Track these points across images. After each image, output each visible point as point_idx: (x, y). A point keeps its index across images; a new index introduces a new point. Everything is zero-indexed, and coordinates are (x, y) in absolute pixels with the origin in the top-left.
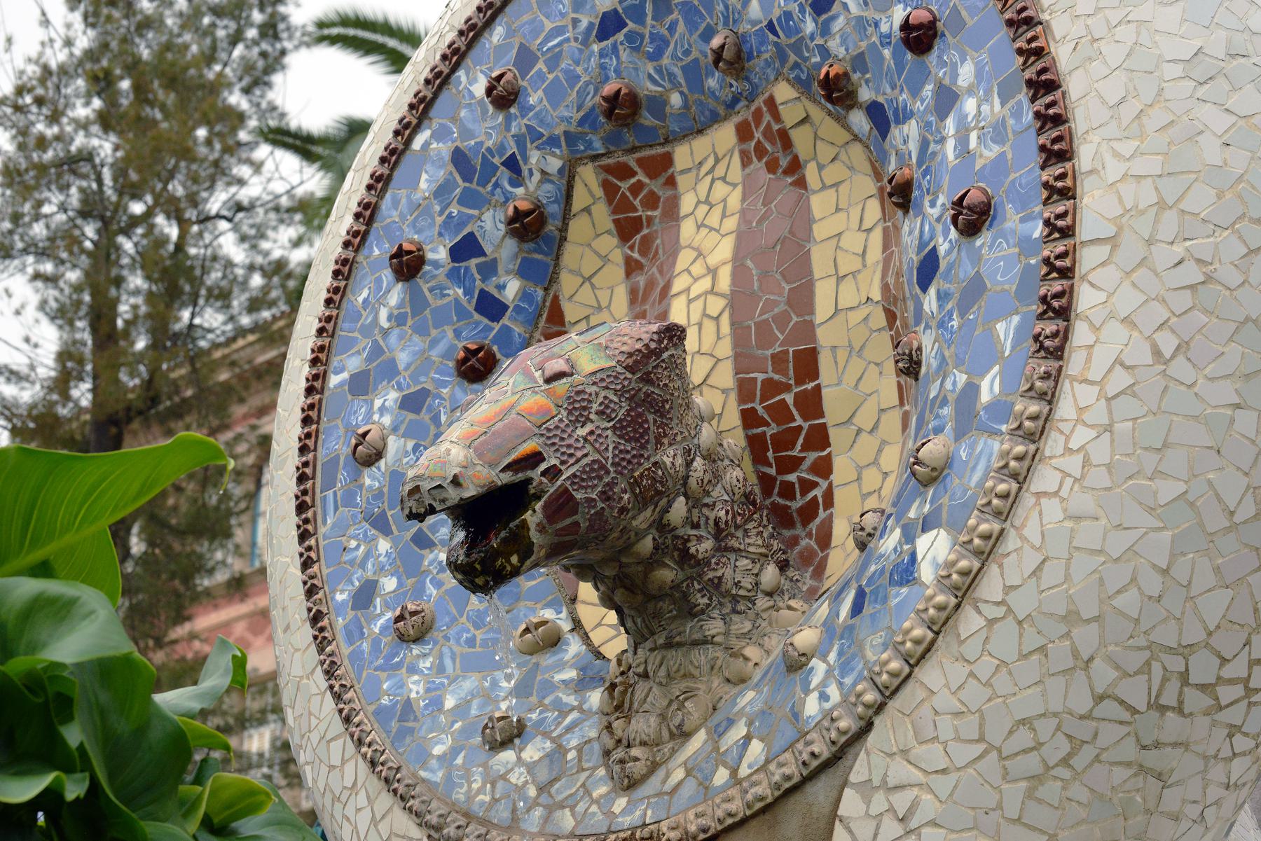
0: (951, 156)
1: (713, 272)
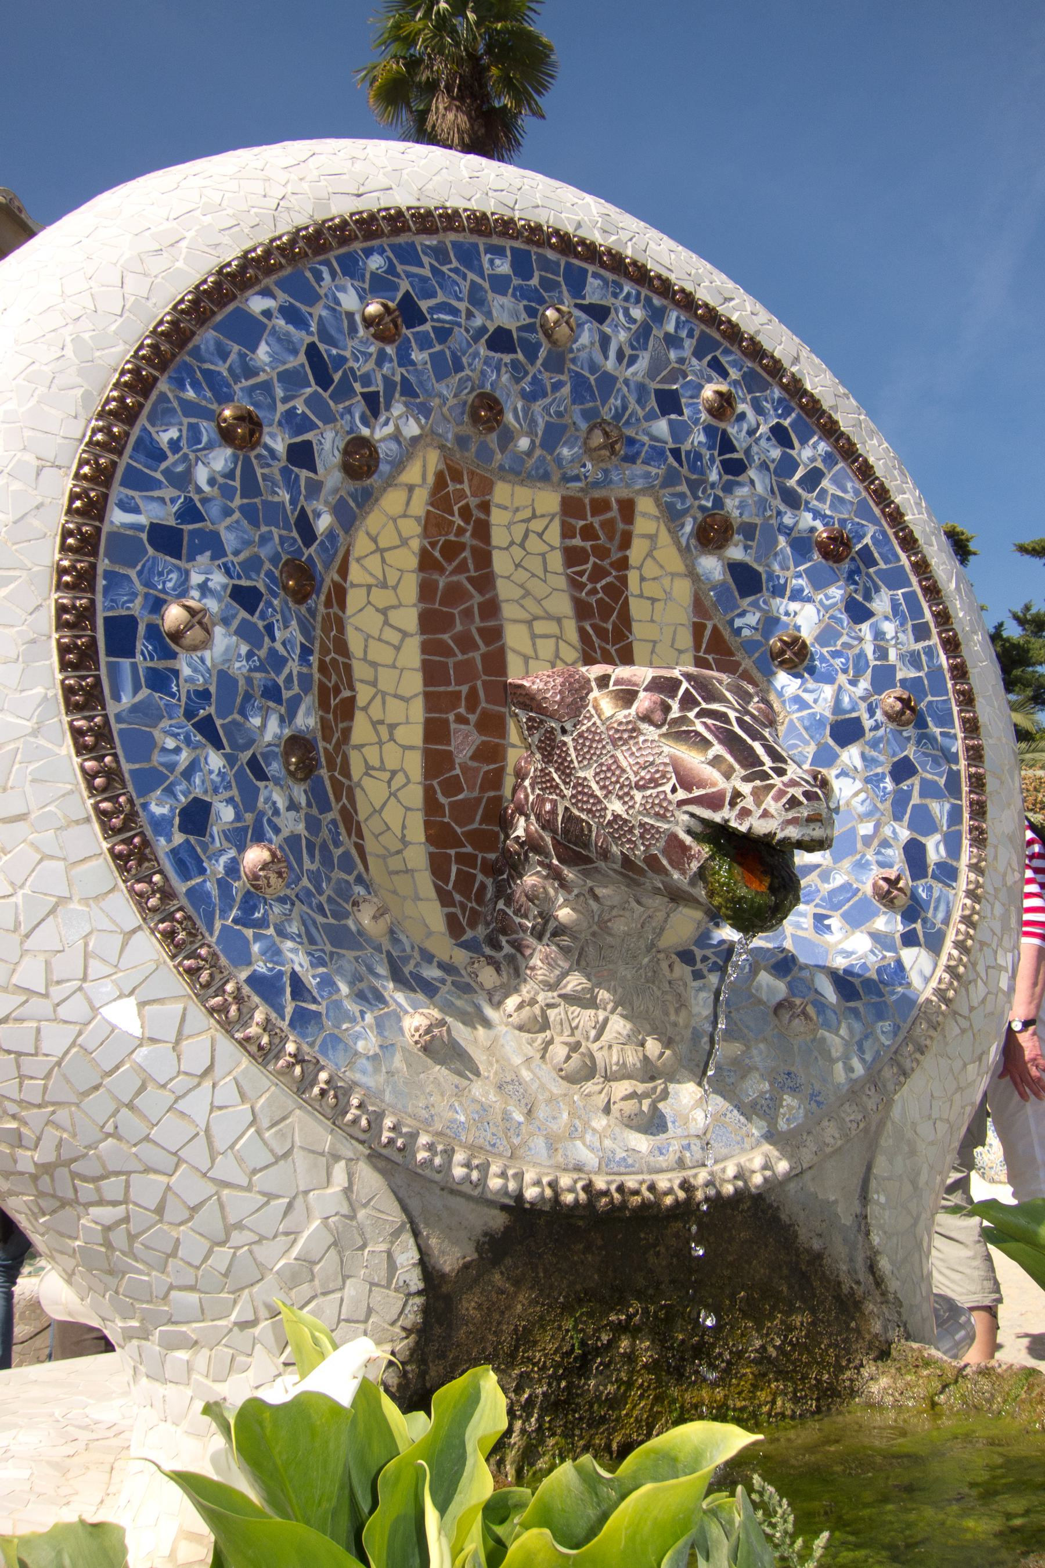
0: (870, 656)
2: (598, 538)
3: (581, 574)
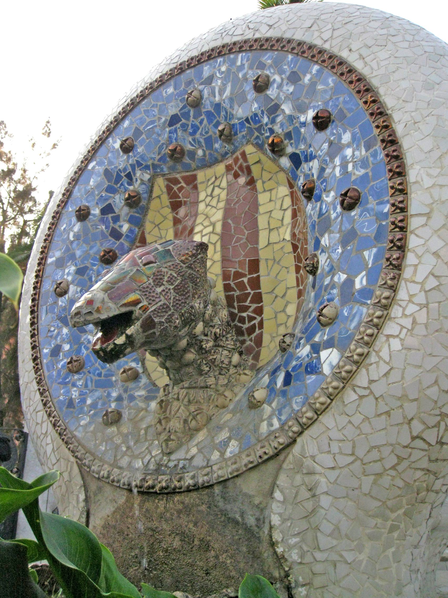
1: (213, 225)
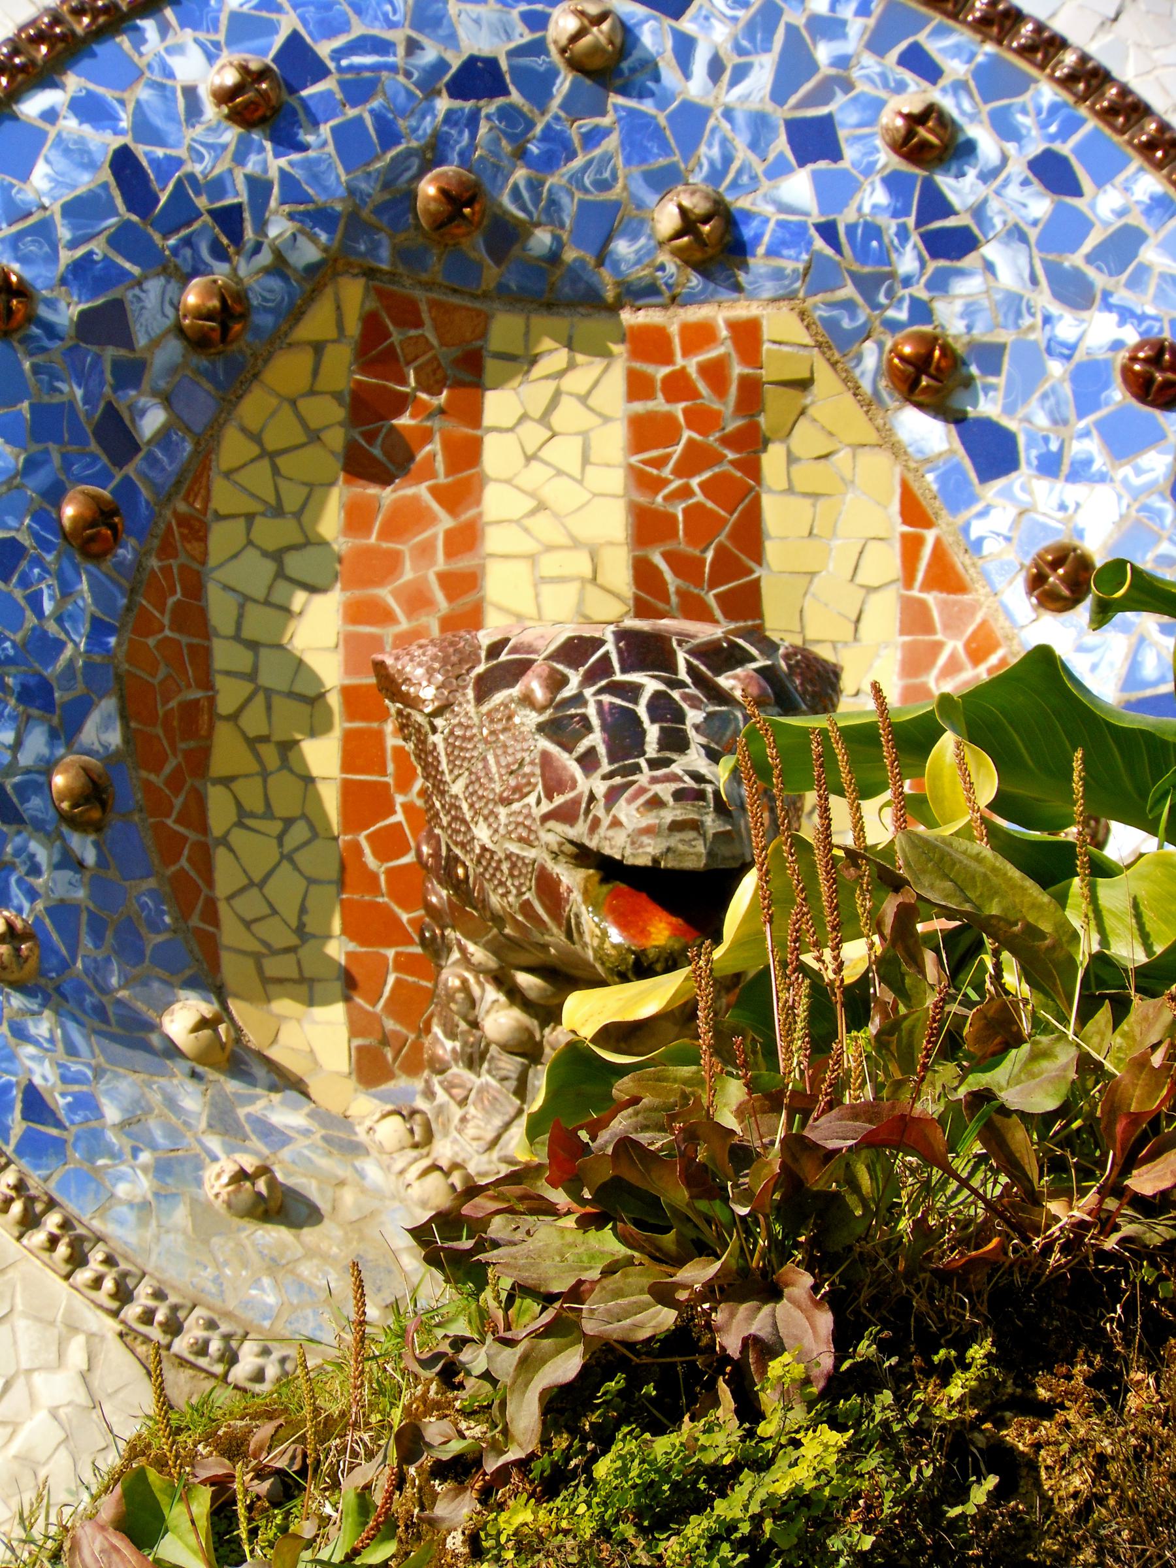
2: (695, 394)
3: (660, 463)
